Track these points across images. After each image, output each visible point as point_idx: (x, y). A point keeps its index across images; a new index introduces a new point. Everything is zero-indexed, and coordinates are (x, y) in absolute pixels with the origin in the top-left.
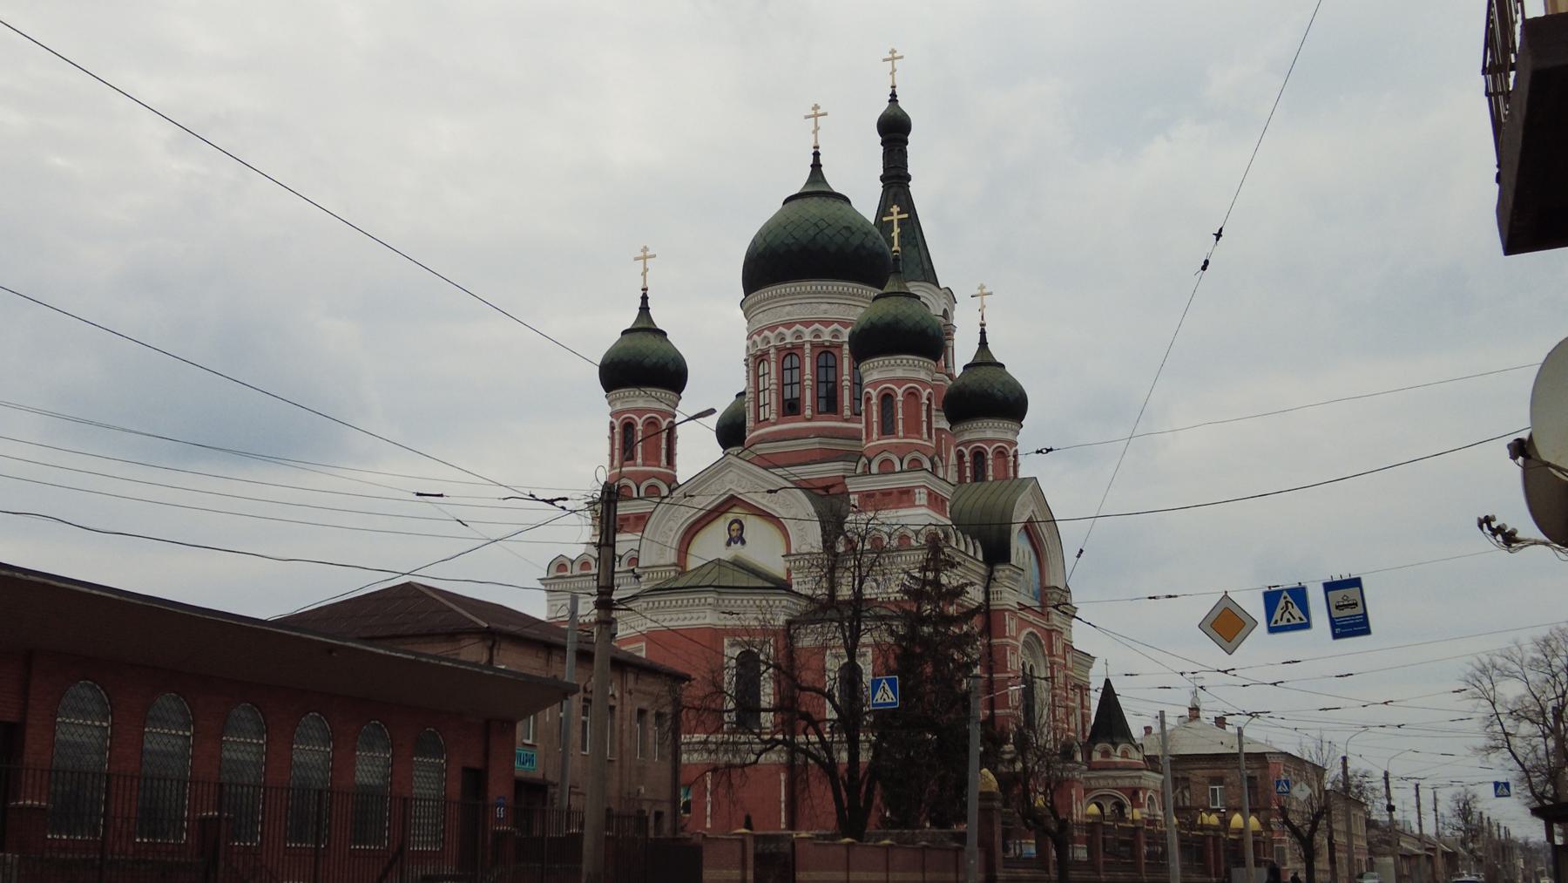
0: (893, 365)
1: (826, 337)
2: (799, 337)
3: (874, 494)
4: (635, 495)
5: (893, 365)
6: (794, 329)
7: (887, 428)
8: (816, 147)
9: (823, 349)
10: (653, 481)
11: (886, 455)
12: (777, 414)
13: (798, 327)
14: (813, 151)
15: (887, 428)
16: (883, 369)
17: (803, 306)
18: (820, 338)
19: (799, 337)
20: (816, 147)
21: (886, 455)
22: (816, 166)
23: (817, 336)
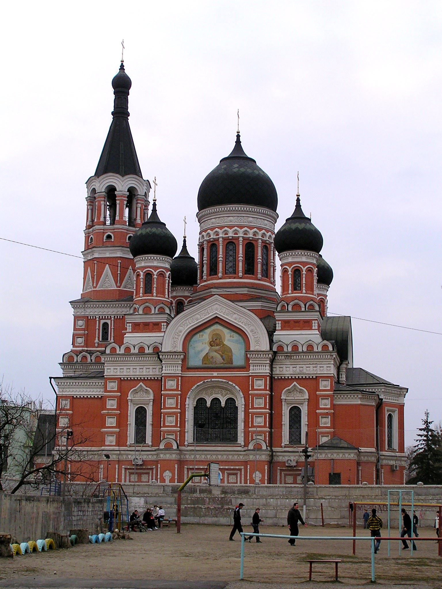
0: (152, 260)
1: (231, 234)
2: (236, 234)
3: (149, 324)
4: (303, 309)
5: (152, 260)
6: (214, 231)
7: (148, 290)
8: (238, 132)
9: (228, 241)
10: (296, 301)
11: (147, 304)
12: (223, 274)
13: (226, 228)
14: (237, 134)
15: (148, 290)
16: (150, 261)
17: (239, 218)
18: (228, 235)
19: (218, 235)
20: (238, 132)
21: (147, 304)
22: (238, 142)
23: (226, 234)
